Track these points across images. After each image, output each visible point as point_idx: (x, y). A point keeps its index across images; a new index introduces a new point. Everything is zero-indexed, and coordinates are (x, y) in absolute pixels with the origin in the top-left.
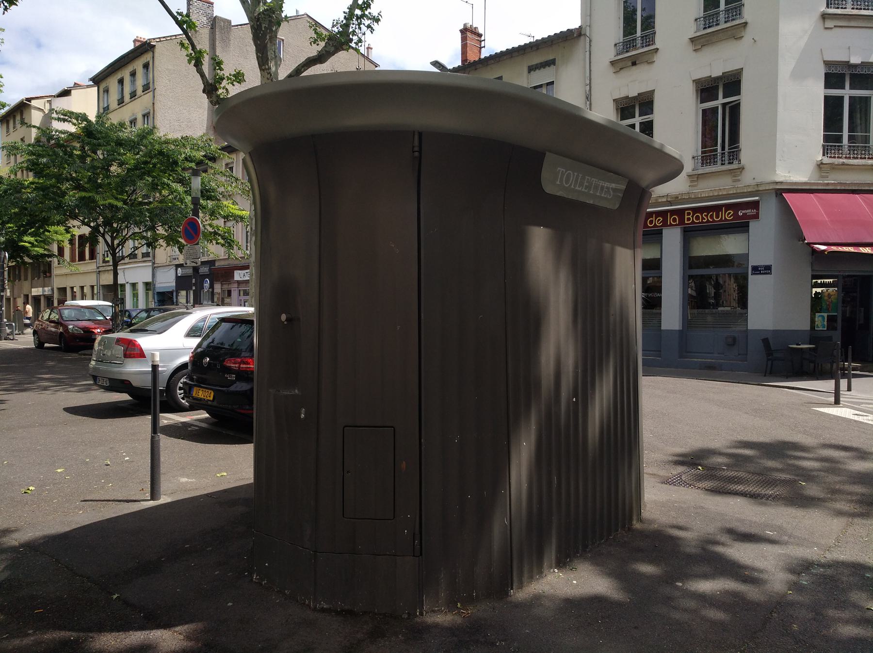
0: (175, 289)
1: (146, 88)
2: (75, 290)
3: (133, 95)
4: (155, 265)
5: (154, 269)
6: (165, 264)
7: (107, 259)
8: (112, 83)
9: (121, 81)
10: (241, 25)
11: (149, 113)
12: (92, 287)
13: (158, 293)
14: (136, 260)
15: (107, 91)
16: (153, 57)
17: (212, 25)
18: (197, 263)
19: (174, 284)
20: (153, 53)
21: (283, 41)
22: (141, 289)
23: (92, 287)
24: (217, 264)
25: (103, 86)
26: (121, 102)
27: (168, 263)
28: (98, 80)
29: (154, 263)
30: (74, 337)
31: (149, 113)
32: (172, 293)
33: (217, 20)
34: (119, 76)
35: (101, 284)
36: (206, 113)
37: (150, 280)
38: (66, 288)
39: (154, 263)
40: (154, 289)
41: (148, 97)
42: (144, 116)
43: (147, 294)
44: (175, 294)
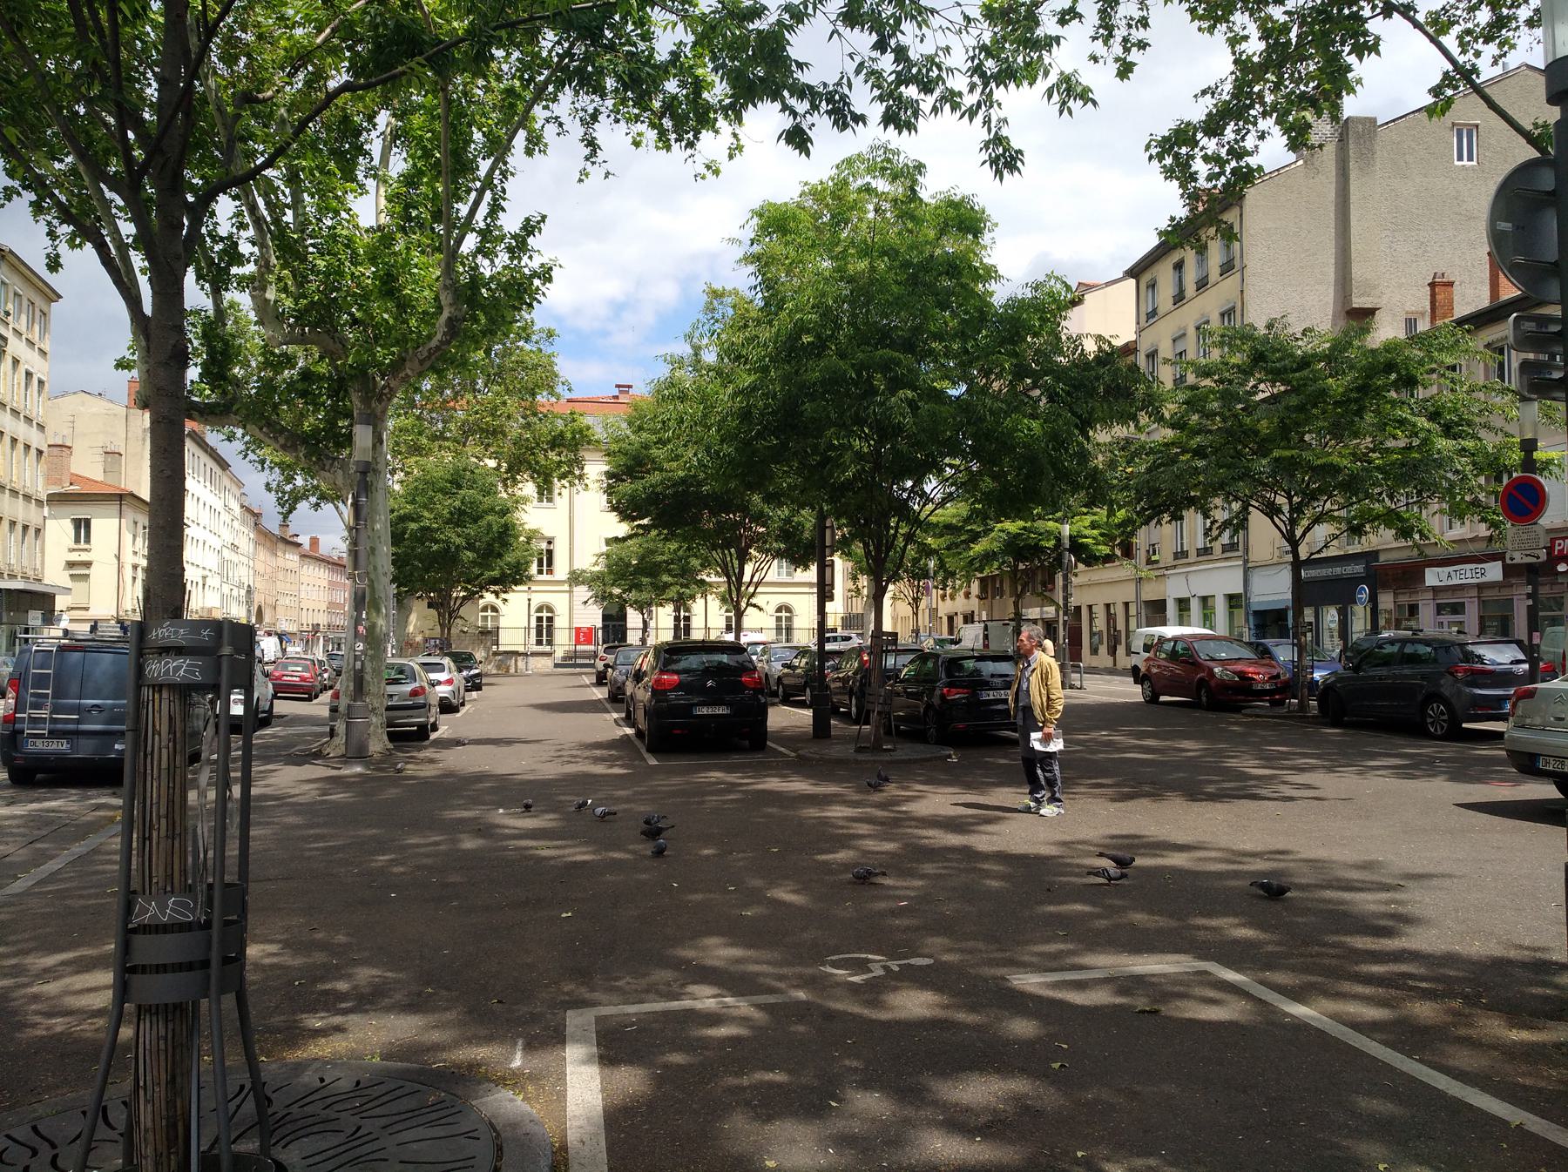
0: (1290, 604)
1: (1227, 268)
2: (1095, 609)
3: (1202, 284)
4: (1250, 565)
5: (1246, 571)
6: (1270, 562)
7: (1153, 558)
8: (1164, 273)
9: (1179, 266)
10: (1393, 121)
11: (1233, 309)
12: (1126, 604)
13: (1256, 613)
14: (1210, 557)
15: (1152, 286)
16: (1241, 215)
17: (1341, 134)
18: (1538, 558)
19: (1289, 596)
20: (1241, 207)
21: (1477, 126)
22: (1220, 607)
23: (1126, 604)
24: (1382, 558)
25: (1146, 278)
26: (1179, 298)
27: (1275, 560)
28: (1135, 272)
29: (1246, 562)
30: (1224, 686)
31: (1233, 309)
32: (1285, 610)
33: (1350, 124)
34: (1175, 257)
35: (1144, 598)
36: (1331, 291)
37: (1239, 590)
38: (1164, 601)
39: (1246, 562)
40: (1248, 605)
41: (1232, 281)
42: (1222, 315)
43: (1231, 615)
44: (1290, 614)
